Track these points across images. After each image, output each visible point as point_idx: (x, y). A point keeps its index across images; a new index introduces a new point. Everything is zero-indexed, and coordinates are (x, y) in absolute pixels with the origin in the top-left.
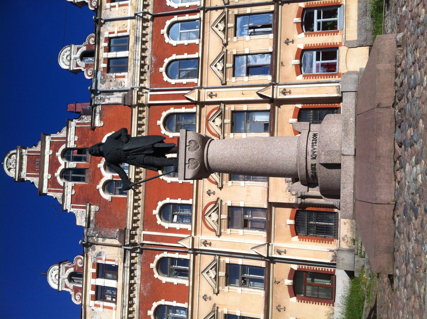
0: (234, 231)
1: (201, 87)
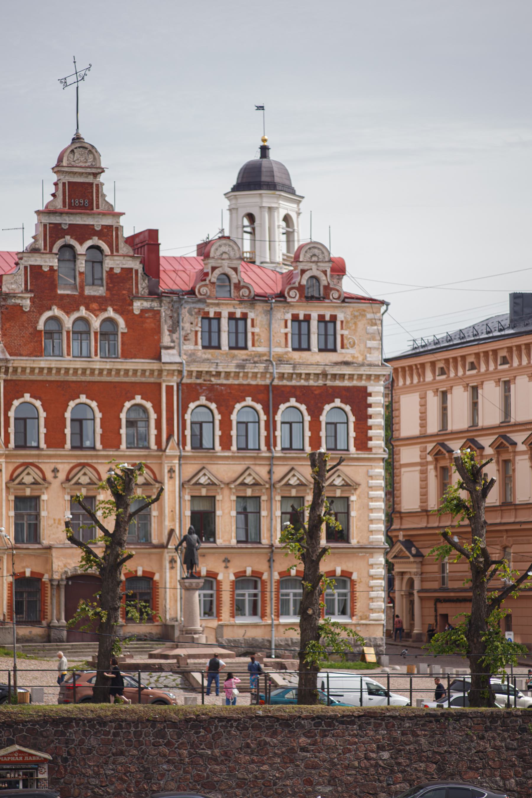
0: (12, 504)
1: (180, 457)
